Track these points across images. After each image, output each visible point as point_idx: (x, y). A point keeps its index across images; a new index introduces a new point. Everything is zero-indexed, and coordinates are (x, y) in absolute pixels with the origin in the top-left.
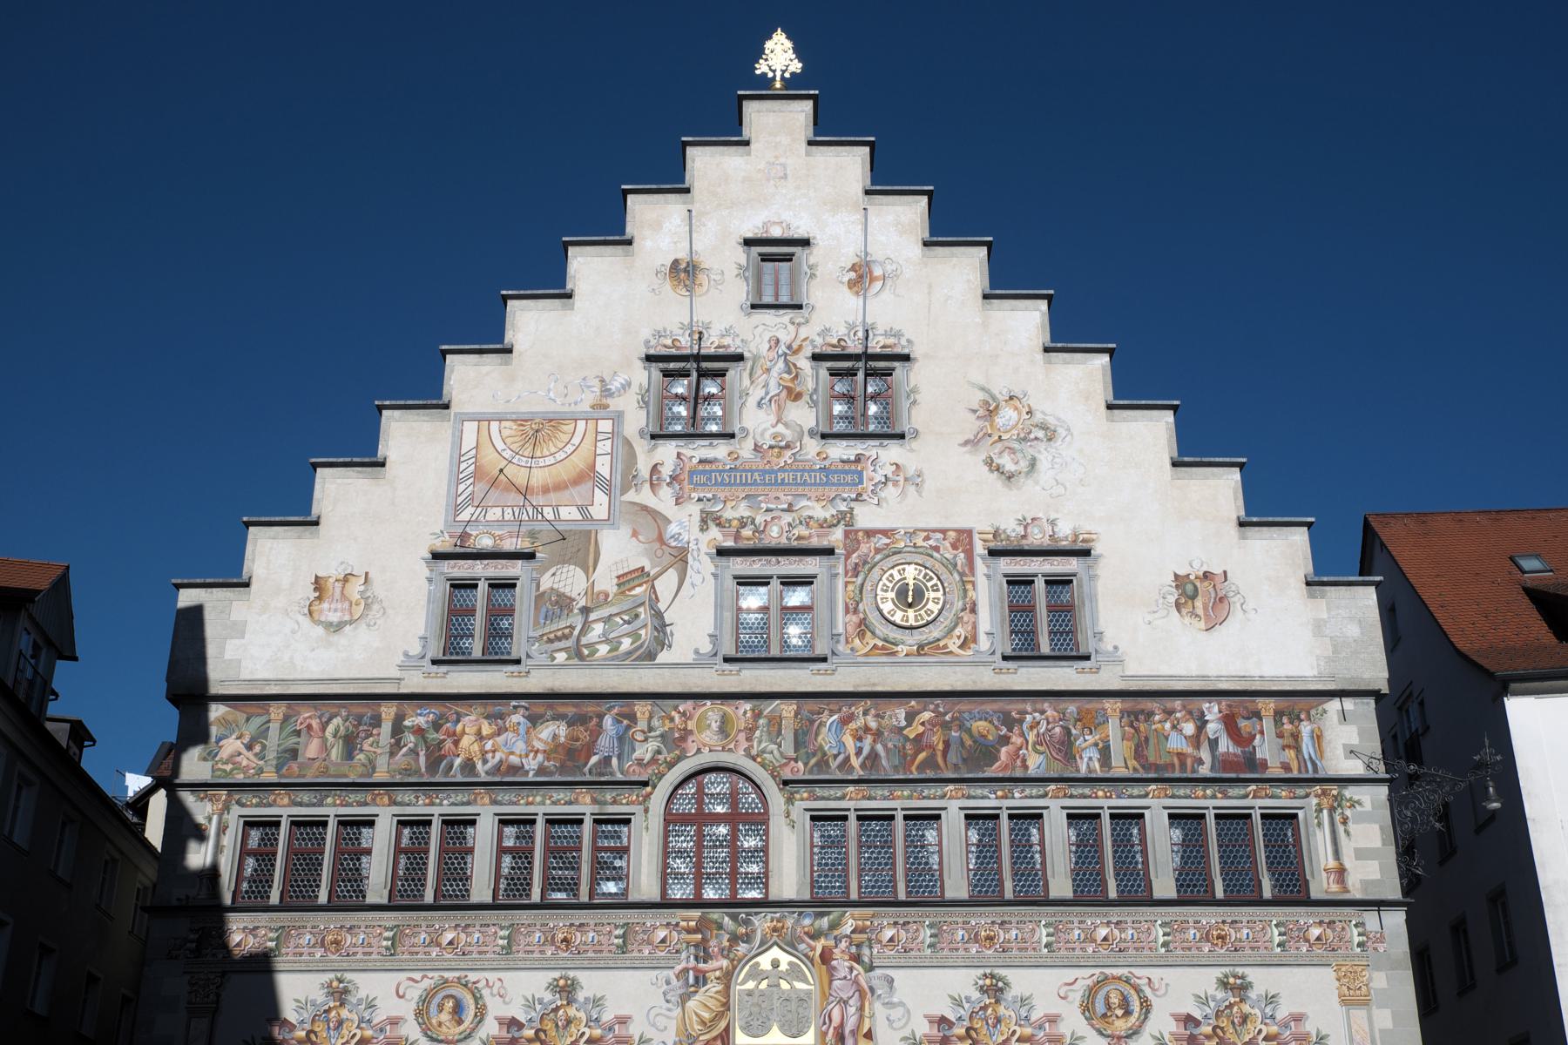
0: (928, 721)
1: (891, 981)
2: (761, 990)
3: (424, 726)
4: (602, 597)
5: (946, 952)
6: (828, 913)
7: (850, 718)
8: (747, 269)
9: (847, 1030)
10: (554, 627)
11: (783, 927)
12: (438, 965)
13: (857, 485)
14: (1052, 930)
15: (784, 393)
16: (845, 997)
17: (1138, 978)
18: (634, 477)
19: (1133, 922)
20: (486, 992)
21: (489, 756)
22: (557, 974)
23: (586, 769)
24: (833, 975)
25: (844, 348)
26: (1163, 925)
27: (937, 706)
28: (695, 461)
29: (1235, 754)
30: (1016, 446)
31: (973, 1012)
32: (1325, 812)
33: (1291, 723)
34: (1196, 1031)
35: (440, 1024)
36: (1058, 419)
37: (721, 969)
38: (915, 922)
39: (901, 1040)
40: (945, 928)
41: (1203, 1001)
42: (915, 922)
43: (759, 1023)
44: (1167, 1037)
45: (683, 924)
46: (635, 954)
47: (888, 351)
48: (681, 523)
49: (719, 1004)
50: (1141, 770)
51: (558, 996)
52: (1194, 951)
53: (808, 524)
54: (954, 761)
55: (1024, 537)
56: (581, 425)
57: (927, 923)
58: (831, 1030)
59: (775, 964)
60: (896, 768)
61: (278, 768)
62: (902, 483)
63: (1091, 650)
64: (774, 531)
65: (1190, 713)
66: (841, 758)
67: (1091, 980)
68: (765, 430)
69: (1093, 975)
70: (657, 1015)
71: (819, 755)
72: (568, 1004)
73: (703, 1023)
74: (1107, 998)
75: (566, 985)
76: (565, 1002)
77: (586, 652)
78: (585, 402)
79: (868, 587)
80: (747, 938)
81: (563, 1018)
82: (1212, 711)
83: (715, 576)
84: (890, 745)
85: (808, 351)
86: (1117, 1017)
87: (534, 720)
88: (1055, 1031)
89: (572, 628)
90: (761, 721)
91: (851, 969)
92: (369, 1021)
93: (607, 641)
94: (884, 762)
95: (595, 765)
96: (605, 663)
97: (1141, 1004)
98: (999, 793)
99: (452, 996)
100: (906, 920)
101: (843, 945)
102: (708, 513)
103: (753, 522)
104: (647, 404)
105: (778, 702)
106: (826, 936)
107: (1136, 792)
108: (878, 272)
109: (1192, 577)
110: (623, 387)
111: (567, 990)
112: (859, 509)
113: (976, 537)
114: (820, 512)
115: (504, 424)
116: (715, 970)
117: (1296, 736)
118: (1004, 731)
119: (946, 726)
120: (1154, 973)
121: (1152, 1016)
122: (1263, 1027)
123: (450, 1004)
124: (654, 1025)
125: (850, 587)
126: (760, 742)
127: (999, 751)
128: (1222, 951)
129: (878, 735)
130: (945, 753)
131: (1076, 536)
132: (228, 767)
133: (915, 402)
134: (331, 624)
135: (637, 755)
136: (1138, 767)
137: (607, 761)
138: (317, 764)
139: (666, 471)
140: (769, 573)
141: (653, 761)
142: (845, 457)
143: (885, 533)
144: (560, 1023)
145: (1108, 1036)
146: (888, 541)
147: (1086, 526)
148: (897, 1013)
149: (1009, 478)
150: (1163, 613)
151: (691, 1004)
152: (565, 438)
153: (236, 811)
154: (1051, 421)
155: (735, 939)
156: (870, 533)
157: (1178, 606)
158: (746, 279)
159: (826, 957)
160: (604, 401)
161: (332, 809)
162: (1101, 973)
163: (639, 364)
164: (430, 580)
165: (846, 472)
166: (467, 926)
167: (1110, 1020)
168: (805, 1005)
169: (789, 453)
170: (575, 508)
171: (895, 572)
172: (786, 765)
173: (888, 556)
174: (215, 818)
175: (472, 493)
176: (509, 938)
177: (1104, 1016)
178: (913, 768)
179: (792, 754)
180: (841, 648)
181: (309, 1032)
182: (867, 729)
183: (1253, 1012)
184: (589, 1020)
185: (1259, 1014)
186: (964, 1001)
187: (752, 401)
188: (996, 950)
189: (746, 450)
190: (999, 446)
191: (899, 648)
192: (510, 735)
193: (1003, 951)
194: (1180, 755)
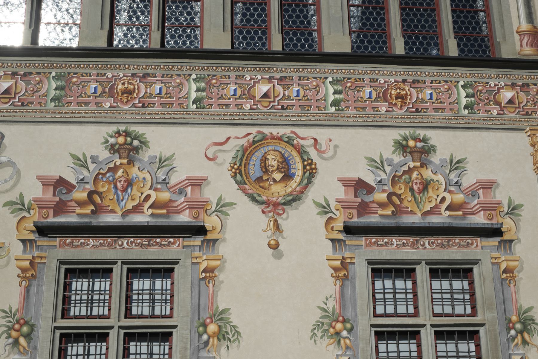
5: (72, 107)
14: (203, 84)
17: (303, 139)
19: (300, 79)
31: (99, 174)
34: (368, 199)
38: (38, 73)
39: (5, 205)
40: (75, 80)
42: (38, 73)
44: (333, 204)
52: (369, 111)
57: (54, 74)
67: (246, 139)
69: (249, 134)
74: (264, 159)
86: (275, 181)
88: (197, 196)
97: (304, 167)
120: (322, 134)
121: (317, 181)
122: (446, 195)
128: (401, 112)
145: (263, 203)
162: (259, 132)
167: (266, 184)
177: (259, 180)
183: (435, 178)
185: (442, 181)
186: (89, 161)
188: (134, 105)
193: (143, 106)
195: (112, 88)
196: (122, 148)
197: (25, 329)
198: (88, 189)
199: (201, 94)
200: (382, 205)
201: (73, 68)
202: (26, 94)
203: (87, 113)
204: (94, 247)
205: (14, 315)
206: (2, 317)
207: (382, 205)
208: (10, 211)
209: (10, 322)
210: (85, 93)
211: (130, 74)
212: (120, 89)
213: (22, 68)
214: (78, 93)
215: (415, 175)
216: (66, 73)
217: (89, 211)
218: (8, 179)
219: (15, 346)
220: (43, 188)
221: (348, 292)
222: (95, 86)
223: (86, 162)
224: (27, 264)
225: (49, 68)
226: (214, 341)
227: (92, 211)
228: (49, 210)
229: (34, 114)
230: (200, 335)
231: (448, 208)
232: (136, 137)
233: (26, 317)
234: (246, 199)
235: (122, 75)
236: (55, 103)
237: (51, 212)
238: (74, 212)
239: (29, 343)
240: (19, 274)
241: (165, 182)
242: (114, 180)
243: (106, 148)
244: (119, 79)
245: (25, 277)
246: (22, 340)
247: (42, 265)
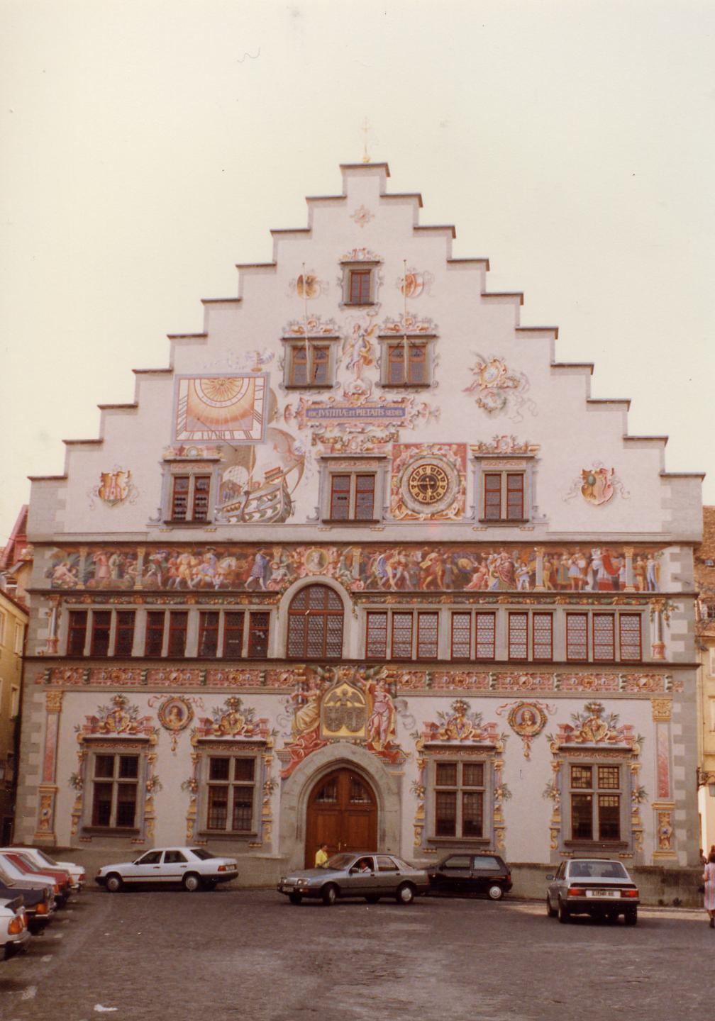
0: (435, 559)
1: (406, 704)
3: (160, 560)
4: (257, 485)
5: (436, 688)
7: (391, 556)
8: (342, 281)
9: (382, 729)
10: (230, 503)
12: (169, 690)
13: (400, 416)
14: (495, 678)
15: (362, 361)
16: (381, 711)
18: (276, 413)
20: (193, 705)
21: (195, 576)
22: (230, 696)
23: (246, 585)
25: (398, 331)
26: (557, 676)
27: (439, 550)
28: (310, 403)
29: (607, 579)
30: (495, 391)
32: (657, 613)
33: (642, 560)
34: (571, 734)
35: (171, 721)
36: (522, 374)
41: (576, 717)
44: (554, 736)
45: (296, 671)
47: (423, 333)
48: (301, 441)
50: (552, 588)
53: (372, 441)
54: (447, 581)
55: (496, 448)
56: (246, 380)
60: (414, 585)
61: (85, 582)
62: (427, 415)
63: (530, 519)
64: (353, 446)
65: (584, 554)
66: (385, 579)
68: (351, 383)
71: (373, 577)
75: (235, 702)
77: (247, 517)
78: (249, 365)
79: (405, 479)
80: (330, 679)
82: (597, 554)
83: (319, 472)
84: (412, 572)
85: (377, 333)
87: (219, 556)
89: (240, 503)
90: (342, 558)
91: (385, 696)
92: (135, 718)
93: (259, 511)
94: (408, 582)
95: (251, 582)
96: (256, 525)
98: (471, 601)
99: (177, 707)
101: (382, 683)
102: (316, 435)
103: (342, 440)
104: (283, 367)
105: (350, 547)
106: (372, 678)
107: (548, 600)
108: (420, 280)
109: (593, 472)
110: (270, 357)
111: (235, 705)
112: (402, 432)
113: (469, 449)
114: (380, 433)
115: (203, 381)
117: (644, 568)
118: (476, 564)
119: (444, 562)
121: (547, 725)
122: (609, 733)
123: (175, 711)
124: (281, 725)
125: (395, 479)
126: (340, 570)
127: (472, 576)
129: (406, 566)
130: (443, 576)
131: (526, 446)
132: (60, 582)
133: (437, 365)
134: (110, 501)
135: (273, 577)
136: (551, 586)
137: (256, 581)
138: (105, 580)
139: (294, 409)
140: (350, 470)
141: (282, 580)
142: (395, 400)
143: (417, 446)
146: (417, 451)
147: (533, 441)
148: (408, 721)
149: (490, 411)
150: (574, 494)
151: (300, 713)
152: (237, 389)
153: (64, 605)
154: (518, 376)
155: (323, 679)
156: (407, 446)
157: (584, 490)
158: (342, 287)
159: (372, 690)
160: (259, 366)
161: (113, 606)
163: (280, 343)
164: (163, 475)
165: (396, 409)
166: (183, 670)
169: (363, 398)
170: (242, 433)
171: (420, 470)
172: (354, 583)
173: (417, 460)
174: (54, 609)
175: (186, 423)
176: (205, 676)
177: (521, 724)
178: (424, 586)
179: (358, 577)
180: (388, 515)
181: (106, 723)
182: (399, 563)
184: (247, 720)
185: (607, 725)
187: (343, 365)
189: (338, 395)
190: (485, 392)
191: (421, 516)
192: (205, 565)
194: (576, 580)
195: (454, 679)
199: (495, 682)
200: (577, 737)
207: (577, 737)
215: (593, 722)
221: (560, 777)
226: (500, 797)
230: (495, 794)
231: (609, 739)
232: (465, 704)
234: (515, 734)
241: (478, 725)
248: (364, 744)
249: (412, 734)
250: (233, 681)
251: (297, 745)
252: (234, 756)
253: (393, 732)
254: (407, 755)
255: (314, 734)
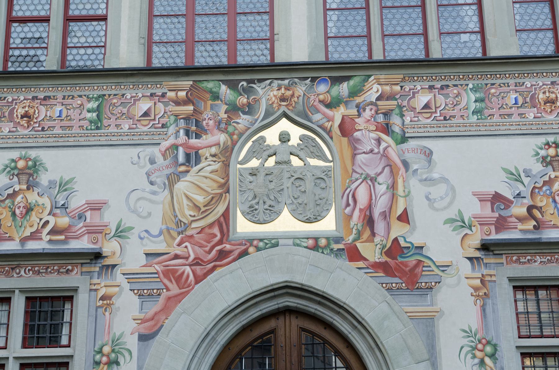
1: (429, 154)
2: (268, 168)
5: (496, 119)
6: (348, 78)
11: (293, 96)
16: (372, 174)
22: (15, 154)
24: (355, 149)
31: (534, 188)
37: (218, 144)
38: (455, 86)
39: (446, 222)
40: (493, 91)
42: (455, 86)
43: (266, 207)
45: (171, 94)
46: (113, 129)
49: (215, 185)
51: (16, 179)
57: (471, 86)
58: (357, 213)
59: (284, 138)
70: (139, 199)
72: (28, 189)
73: (197, 207)
75: (27, 167)
76: (24, 187)
81: (22, 205)
91: (379, 141)
100: (444, 83)
101: (368, 113)
106: (346, 103)
116: (211, 146)
124: (134, 211)
144: (18, 212)
148: (438, 191)
151: (181, 186)
168: (323, 185)
186: (522, 175)
195: (533, 97)
196: (554, 160)
197: (489, 349)
198: (526, 204)
201: (489, 78)
202: (447, 108)
203: (512, 125)
204: (542, 263)
205: (475, 335)
206: (464, 337)
208: (452, 228)
209: (473, 342)
210: (506, 104)
211: (550, 83)
212: (541, 99)
213: (438, 81)
214: (498, 104)
216: (483, 84)
217: (531, 227)
218: (444, 196)
219: (483, 367)
220: (481, 205)
222: (515, 96)
223: (520, 176)
224: (478, 282)
225: (465, 80)
227: (534, 226)
228: (490, 226)
229: (458, 129)
233: (488, 337)
235: (541, 84)
236: (478, 116)
237: (493, 228)
238: (516, 228)
239: (495, 363)
240: (472, 293)
242: (551, 193)
243: (537, 160)
244: (539, 88)
245: (479, 296)
246: (487, 360)
247: (493, 284)
248: (336, 247)
249: (451, 221)
250: (24, 122)
251: (176, 257)
252: (22, 291)
253: (404, 218)
254: (444, 267)
255: (216, 231)
